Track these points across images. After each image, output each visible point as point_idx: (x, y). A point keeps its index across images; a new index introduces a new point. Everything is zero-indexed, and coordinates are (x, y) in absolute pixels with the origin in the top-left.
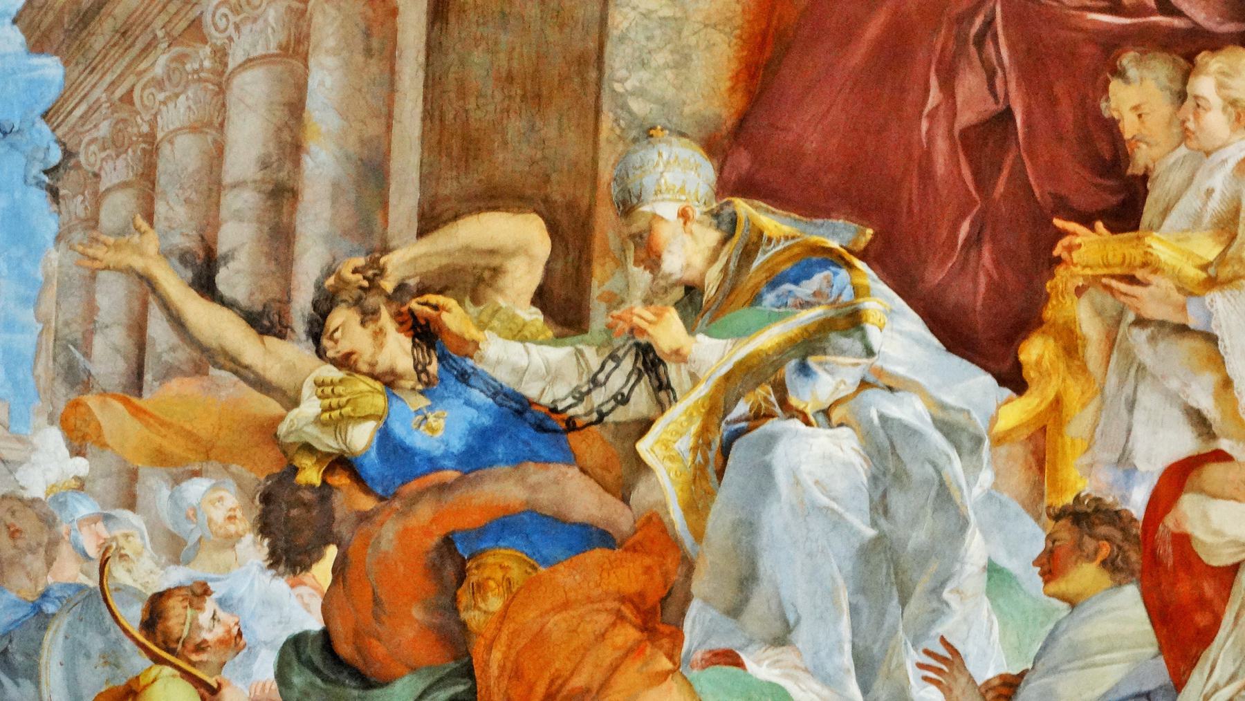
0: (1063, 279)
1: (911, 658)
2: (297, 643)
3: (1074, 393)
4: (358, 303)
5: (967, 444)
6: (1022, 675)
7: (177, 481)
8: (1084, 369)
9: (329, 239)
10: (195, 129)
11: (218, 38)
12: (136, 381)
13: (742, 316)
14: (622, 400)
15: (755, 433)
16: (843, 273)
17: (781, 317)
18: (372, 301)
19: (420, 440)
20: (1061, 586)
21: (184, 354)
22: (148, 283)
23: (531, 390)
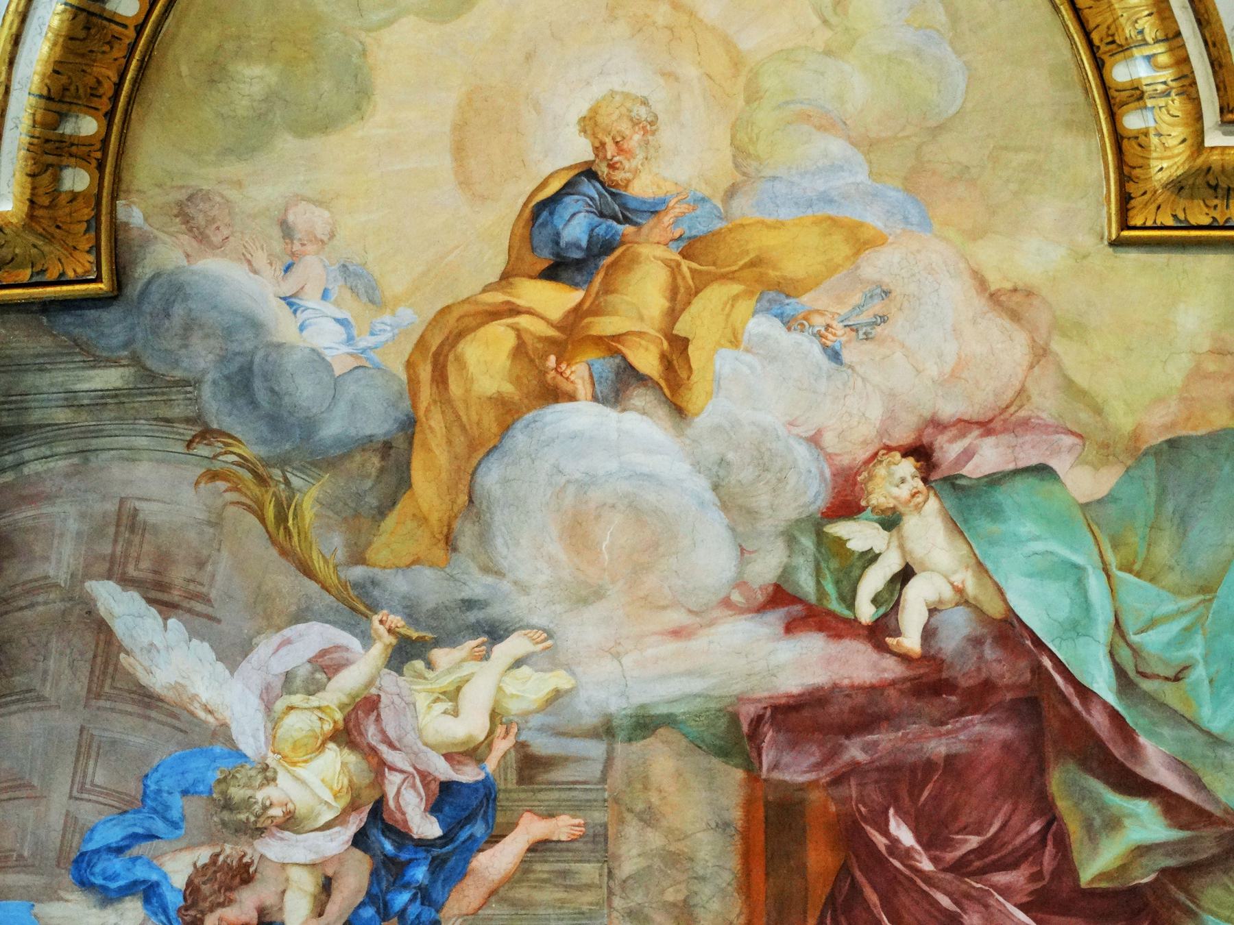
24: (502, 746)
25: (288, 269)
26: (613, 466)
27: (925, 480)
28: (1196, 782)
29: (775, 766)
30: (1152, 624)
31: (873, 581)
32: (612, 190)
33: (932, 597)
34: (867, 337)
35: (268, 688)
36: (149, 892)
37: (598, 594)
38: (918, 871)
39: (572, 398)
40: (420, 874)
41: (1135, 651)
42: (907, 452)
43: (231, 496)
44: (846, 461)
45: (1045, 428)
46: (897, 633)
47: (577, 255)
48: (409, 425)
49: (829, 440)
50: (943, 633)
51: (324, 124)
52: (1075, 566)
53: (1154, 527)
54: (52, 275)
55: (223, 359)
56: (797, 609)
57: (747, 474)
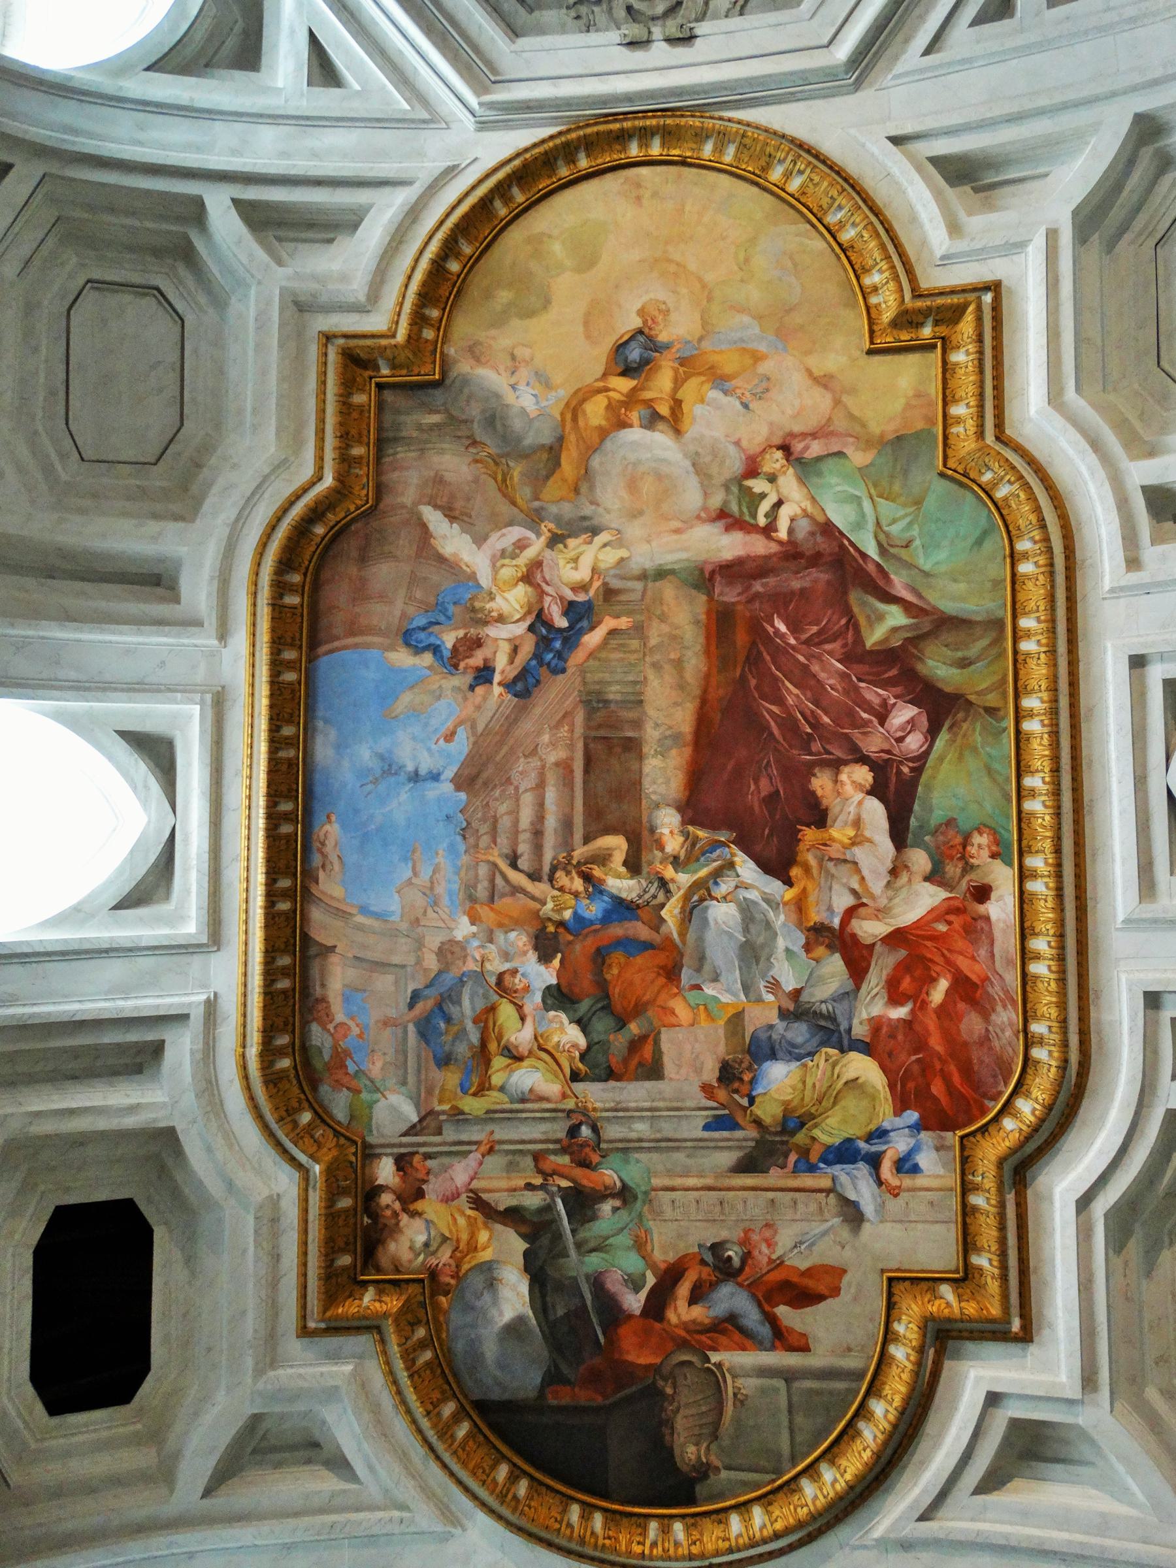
0: (802, 847)
1: (762, 984)
2: (548, 988)
3: (810, 886)
4: (564, 869)
5: (774, 906)
7: (506, 932)
8: (813, 877)
9: (555, 848)
10: (509, 813)
11: (515, 783)
12: (492, 899)
13: (695, 866)
18: (569, 868)
19: (587, 914)
21: (508, 889)
22: (495, 865)
23: (624, 895)
24: (597, 584)
25: (513, 373)
26: (649, 455)
27: (788, 460)
28: (920, 596)
29: (721, 594)
30: (894, 521)
31: (765, 506)
32: (650, 338)
33: (792, 514)
34: (760, 398)
35: (494, 556)
36: (436, 650)
37: (641, 513)
38: (789, 644)
39: (631, 426)
40: (558, 645)
41: (887, 535)
42: (779, 448)
43: (484, 470)
44: (751, 452)
45: (841, 434)
46: (776, 531)
48: (561, 439)
49: (744, 444)
50: (797, 530)
51: (530, 314)
52: (858, 498)
53: (892, 477)
54: (416, 372)
55: (483, 411)
56: (730, 520)
57: (708, 459)
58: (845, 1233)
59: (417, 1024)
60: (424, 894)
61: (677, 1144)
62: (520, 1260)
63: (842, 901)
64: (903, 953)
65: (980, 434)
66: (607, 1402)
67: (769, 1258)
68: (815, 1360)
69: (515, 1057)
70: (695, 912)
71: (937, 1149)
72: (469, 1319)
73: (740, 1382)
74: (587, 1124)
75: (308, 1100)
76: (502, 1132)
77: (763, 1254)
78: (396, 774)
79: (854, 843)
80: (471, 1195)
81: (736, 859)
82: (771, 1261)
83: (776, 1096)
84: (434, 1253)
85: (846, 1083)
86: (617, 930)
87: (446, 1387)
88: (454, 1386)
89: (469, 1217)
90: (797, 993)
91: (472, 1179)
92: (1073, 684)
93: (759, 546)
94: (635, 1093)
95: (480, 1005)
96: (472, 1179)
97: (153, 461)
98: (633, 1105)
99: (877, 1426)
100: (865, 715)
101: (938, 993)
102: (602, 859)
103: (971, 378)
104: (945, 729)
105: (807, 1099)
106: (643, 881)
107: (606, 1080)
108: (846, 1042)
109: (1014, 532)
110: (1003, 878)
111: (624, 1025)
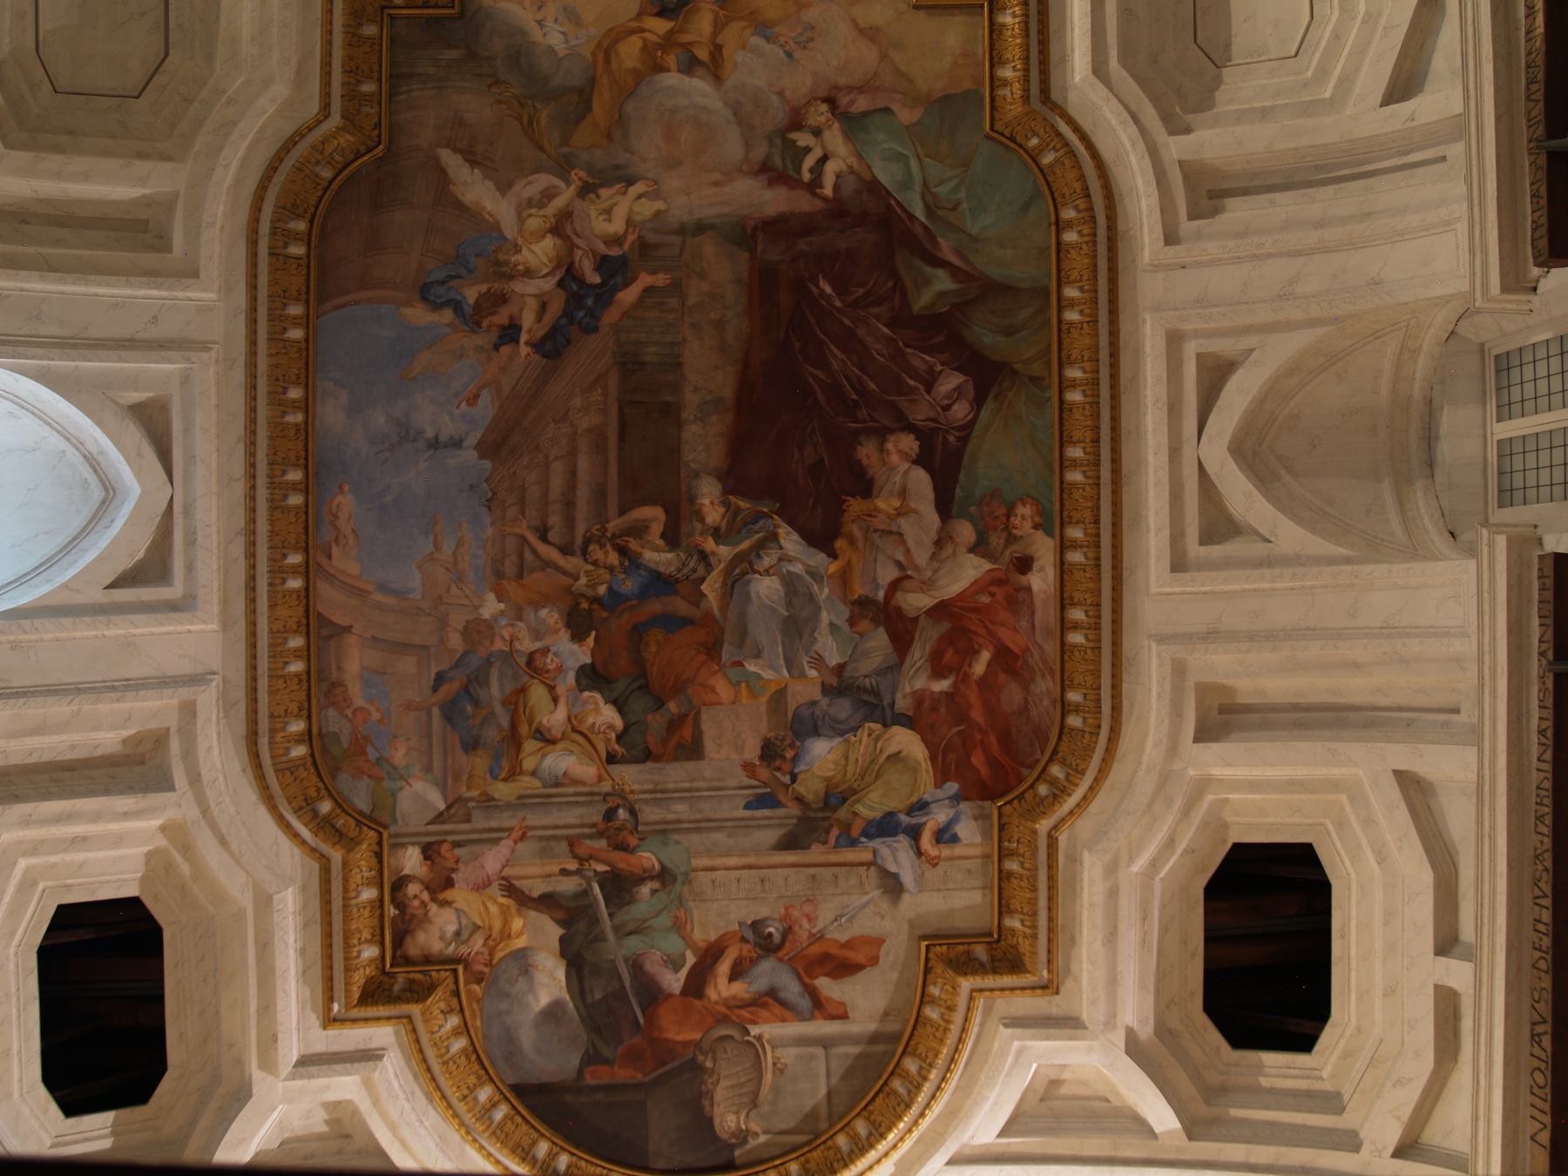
2: (582, 668)
4: (598, 542)
6: (846, 662)
7: (536, 610)
12: (520, 575)
14: (695, 571)
15: (742, 581)
16: (770, 521)
17: (749, 537)
18: (603, 541)
19: (623, 590)
20: (854, 629)
22: (524, 539)
23: (662, 569)
24: (631, 238)
25: (540, 8)
27: (833, 114)
28: (964, 258)
30: (941, 182)
31: (809, 161)
36: (457, 306)
38: (833, 306)
39: (668, 70)
40: (590, 302)
41: (934, 196)
42: (825, 100)
46: (821, 187)
47: (672, 6)
49: (788, 93)
52: (902, 154)
58: (885, 905)
59: (442, 707)
60: (448, 570)
61: (717, 824)
62: (557, 945)
63: (887, 574)
64: (945, 626)
65: (1026, 98)
66: (648, 1079)
67: (810, 932)
68: (852, 1028)
69: (546, 739)
70: (736, 585)
71: (975, 818)
72: (503, 1006)
73: (780, 1052)
74: (624, 806)
75: (327, 788)
76: (534, 819)
77: (803, 931)
78: (414, 440)
79: (901, 513)
80: (503, 882)
81: (781, 531)
82: (811, 935)
83: (819, 773)
84: (466, 942)
85: (889, 757)
86: (655, 606)
87: (482, 1072)
88: (491, 1072)
89: (502, 905)
90: (841, 668)
91: (504, 867)
92: (1114, 355)
93: (803, 203)
94: (675, 774)
95: (510, 687)
96: (504, 867)
97: (136, 94)
98: (671, 786)
99: (911, 1083)
100: (912, 383)
101: (979, 668)
102: (639, 531)
103: (1018, 41)
104: (991, 397)
105: (849, 776)
106: (682, 554)
107: (644, 762)
108: (888, 712)
109: (1059, 200)
110: (1044, 549)
111: (663, 705)
